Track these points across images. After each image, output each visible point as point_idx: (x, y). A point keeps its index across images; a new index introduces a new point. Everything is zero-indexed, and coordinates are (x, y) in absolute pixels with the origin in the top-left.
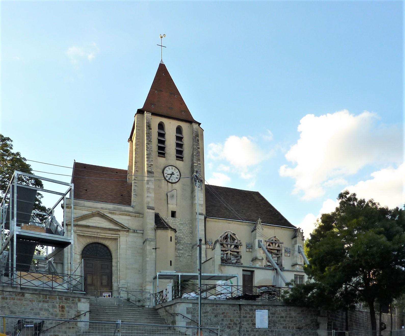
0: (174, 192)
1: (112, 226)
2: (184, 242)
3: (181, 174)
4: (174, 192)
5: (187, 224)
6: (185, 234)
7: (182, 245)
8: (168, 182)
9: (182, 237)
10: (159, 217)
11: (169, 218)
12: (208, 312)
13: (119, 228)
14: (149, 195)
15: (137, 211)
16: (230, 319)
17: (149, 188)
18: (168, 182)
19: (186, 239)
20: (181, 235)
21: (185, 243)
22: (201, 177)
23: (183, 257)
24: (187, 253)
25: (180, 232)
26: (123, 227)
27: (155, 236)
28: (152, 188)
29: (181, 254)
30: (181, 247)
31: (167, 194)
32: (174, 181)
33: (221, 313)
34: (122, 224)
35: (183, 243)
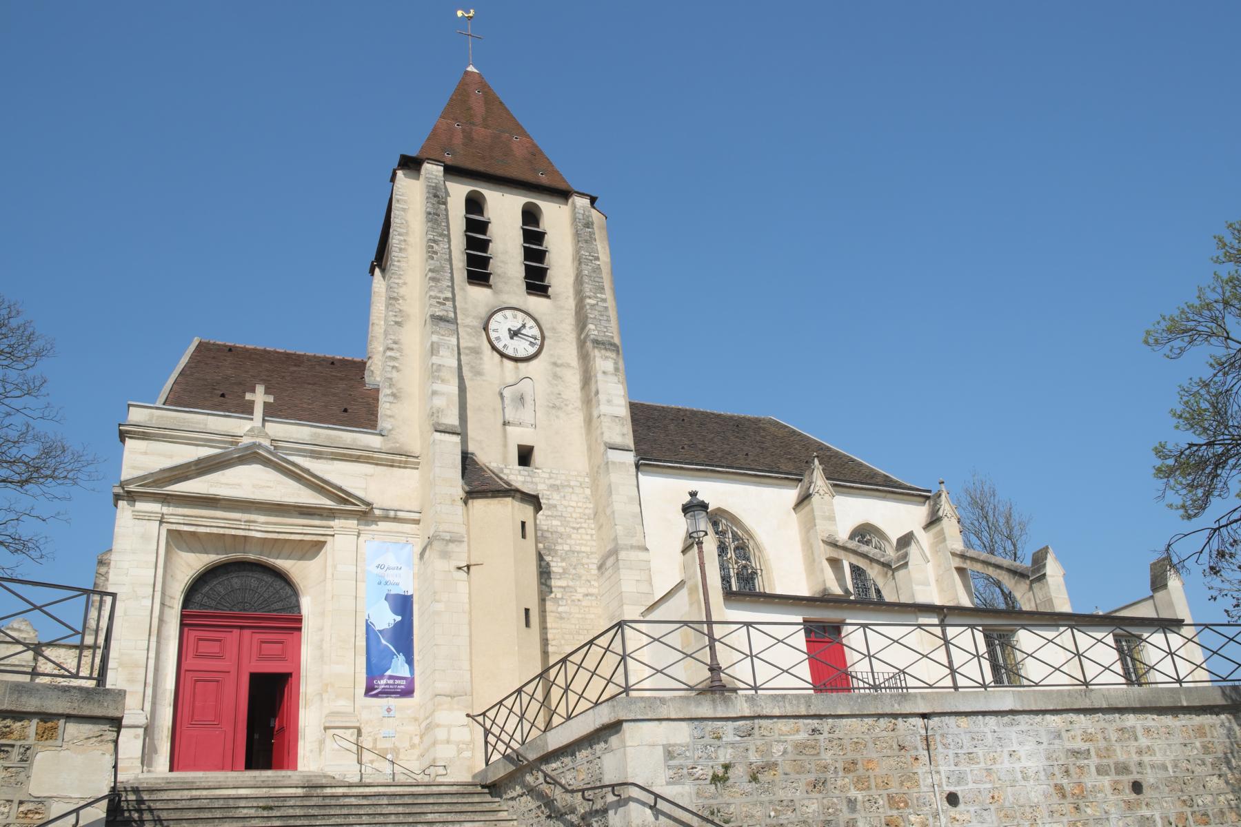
0: (525, 386)
1: (307, 497)
2: (566, 548)
3: (546, 334)
4: (525, 386)
5: (575, 488)
6: (569, 522)
7: (563, 560)
8: (503, 355)
9: (561, 529)
10: (478, 464)
11: (510, 467)
12: (775, 764)
13: (335, 504)
14: (438, 386)
15: (398, 445)
16: (888, 795)
18: (503, 355)
19: (573, 536)
20: (555, 523)
21: (573, 552)
22: (612, 337)
23: (569, 602)
24: (580, 587)
25: (550, 513)
26: (346, 502)
27: (467, 524)
29: (562, 590)
30: (560, 564)
31: (501, 395)
32: (522, 354)
33: (840, 765)
34: (340, 489)
35: (566, 552)
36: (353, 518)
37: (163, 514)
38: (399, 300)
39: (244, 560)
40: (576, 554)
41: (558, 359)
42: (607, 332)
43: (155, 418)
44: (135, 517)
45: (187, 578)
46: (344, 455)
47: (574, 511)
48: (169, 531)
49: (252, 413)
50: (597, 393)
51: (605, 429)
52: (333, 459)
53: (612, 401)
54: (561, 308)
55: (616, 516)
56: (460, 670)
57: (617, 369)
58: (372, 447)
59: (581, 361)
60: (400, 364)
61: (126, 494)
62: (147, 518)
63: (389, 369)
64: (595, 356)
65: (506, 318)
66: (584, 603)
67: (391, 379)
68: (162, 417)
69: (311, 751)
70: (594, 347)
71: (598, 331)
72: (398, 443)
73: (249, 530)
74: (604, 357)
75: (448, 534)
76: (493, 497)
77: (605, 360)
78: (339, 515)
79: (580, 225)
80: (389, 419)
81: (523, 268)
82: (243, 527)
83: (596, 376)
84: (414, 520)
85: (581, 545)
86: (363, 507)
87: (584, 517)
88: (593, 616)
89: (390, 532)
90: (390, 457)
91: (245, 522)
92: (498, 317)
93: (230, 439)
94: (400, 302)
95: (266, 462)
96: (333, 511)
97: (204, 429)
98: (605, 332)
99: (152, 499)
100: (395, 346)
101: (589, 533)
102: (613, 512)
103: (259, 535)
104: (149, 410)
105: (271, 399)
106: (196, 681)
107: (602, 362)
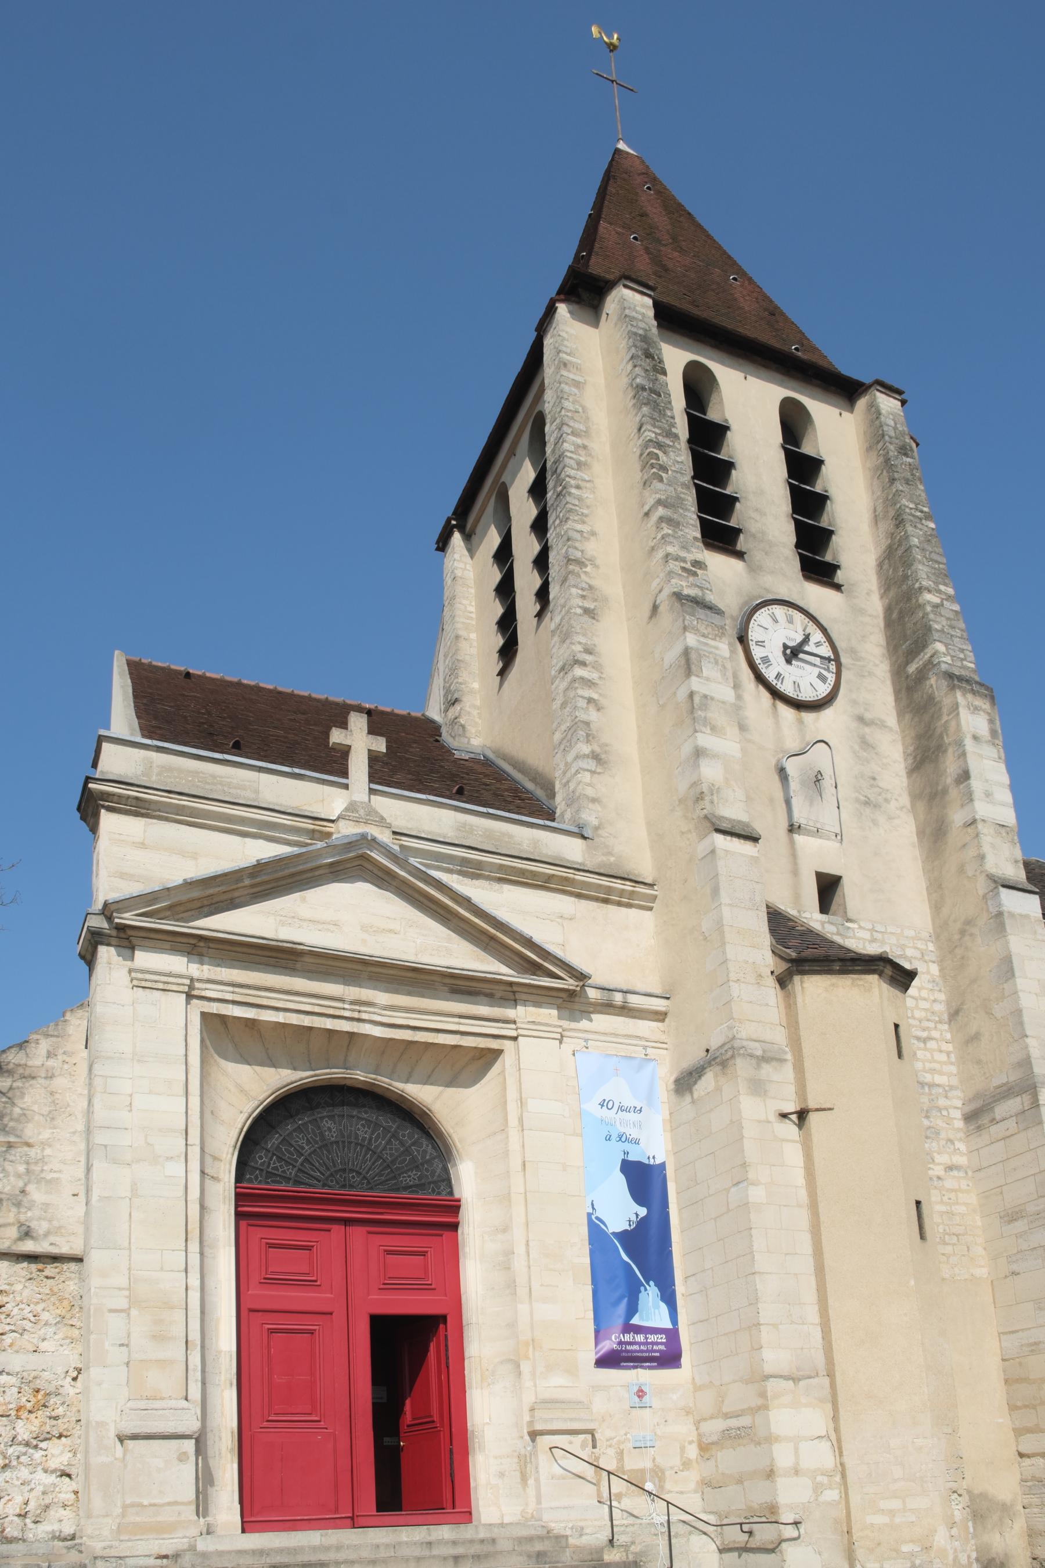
15: (612, 859)
17: (705, 696)
26: (535, 968)
28: (723, 702)
34: (529, 943)
36: (550, 1005)
37: (192, 980)
38: (586, 566)
39: (343, 1083)
40: (927, 1089)
41: (866, 710)
42: (965, 659)
43: (155, 770)
44: (135, 982)
45: (242, 1118)
46: (522, 872)
47: (917, 1005)
48: (204, 1015)
49: (345, 774)
50: (965, 776)
51: (986, 849)
52: (500, 880)
53: (992, 794)
54: (861, 611)
55: (1026, 1019)
56: (803, 1324)
57: (993, 733)
58: (568, 861)
59: (908, 717)
60: (600, 695)
61: (114, 933)
62: (161, 986)
63: (582, 703)
64: (956, 707)
65: (776, 621)
66: (949, 1184)
67: (587, 724)
68: (170, 769)
69: (502, 1475)
70: (952, 688)
71: (952, 657)
72: (610, 854)
73: (359, 1020)
74: (972, 708)
75: (757, 1045)
76: (843, 972)
77: (973, 713)
78: (524, 997)
79: (892, 447)
80: (591, 805)
81: (791, 527)
82: (347, 1014)
83: (960, 743)
84: (656, 1013)
85: (933, 1071)
86: (571, 981)
87: (933, 1018)
88: (962, 1209)
89: (616, 1035)
90: (605, 882)
91: (352, 1003)
92: (762, 617)
93: (308, 825)
94: (588, 569)
95: (383, 879)
96: (515, 989)
97: (255, 800)
98: (962, 660)
99: (167, 945)
100: (588, 658)
101: (943, 1048)
102: (1018, 1013)
103: (378, 1032)
104: (143, 753)
105: (380, 745)
106: (271, 1331)
107: (970, 717)
